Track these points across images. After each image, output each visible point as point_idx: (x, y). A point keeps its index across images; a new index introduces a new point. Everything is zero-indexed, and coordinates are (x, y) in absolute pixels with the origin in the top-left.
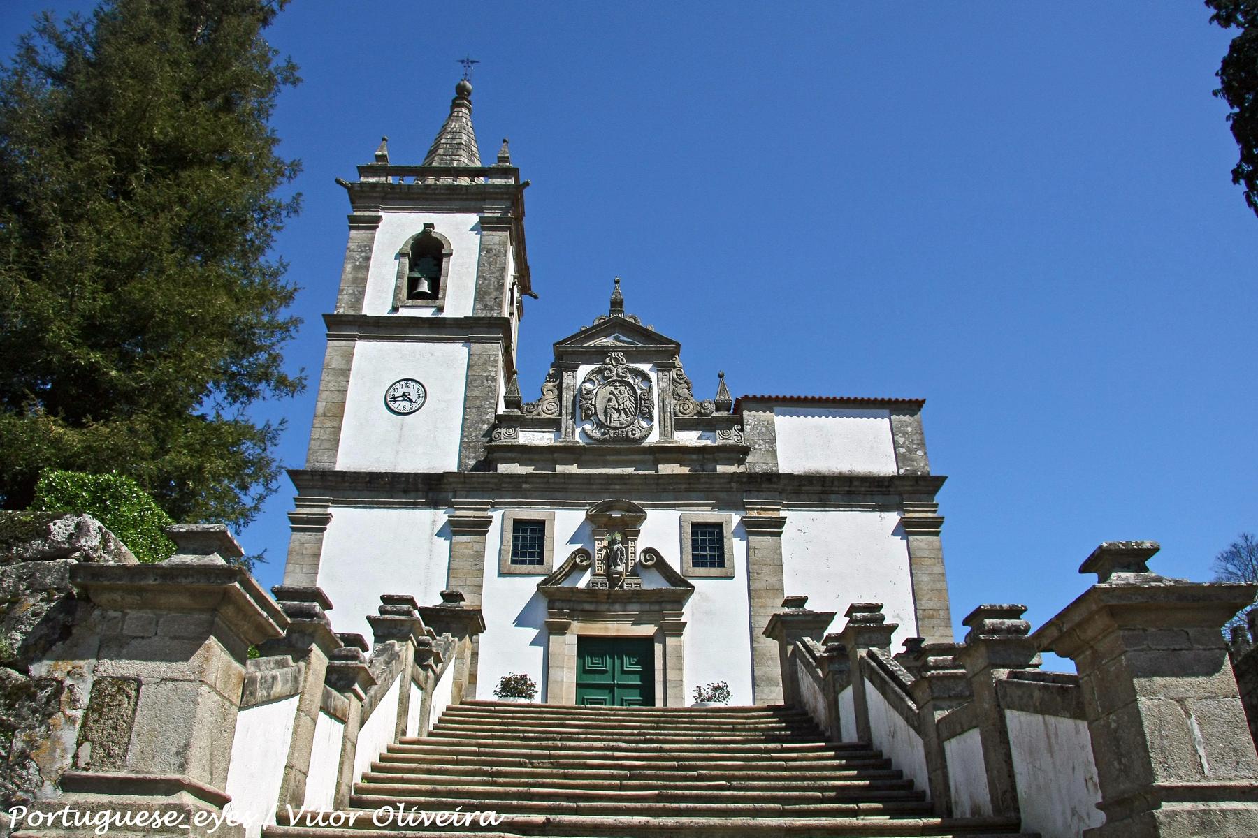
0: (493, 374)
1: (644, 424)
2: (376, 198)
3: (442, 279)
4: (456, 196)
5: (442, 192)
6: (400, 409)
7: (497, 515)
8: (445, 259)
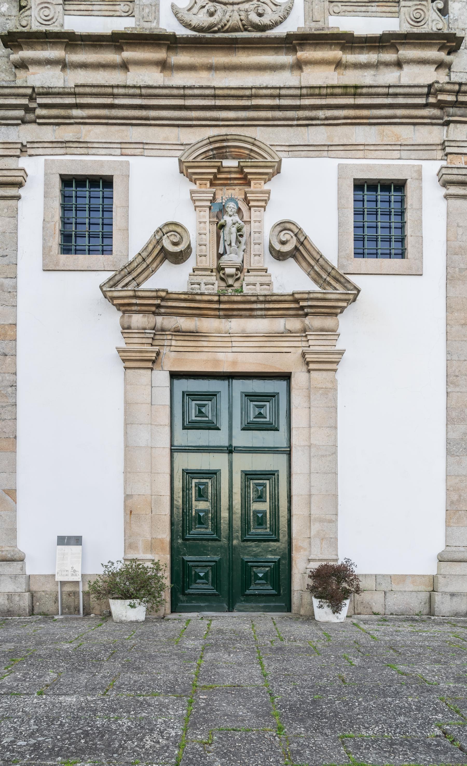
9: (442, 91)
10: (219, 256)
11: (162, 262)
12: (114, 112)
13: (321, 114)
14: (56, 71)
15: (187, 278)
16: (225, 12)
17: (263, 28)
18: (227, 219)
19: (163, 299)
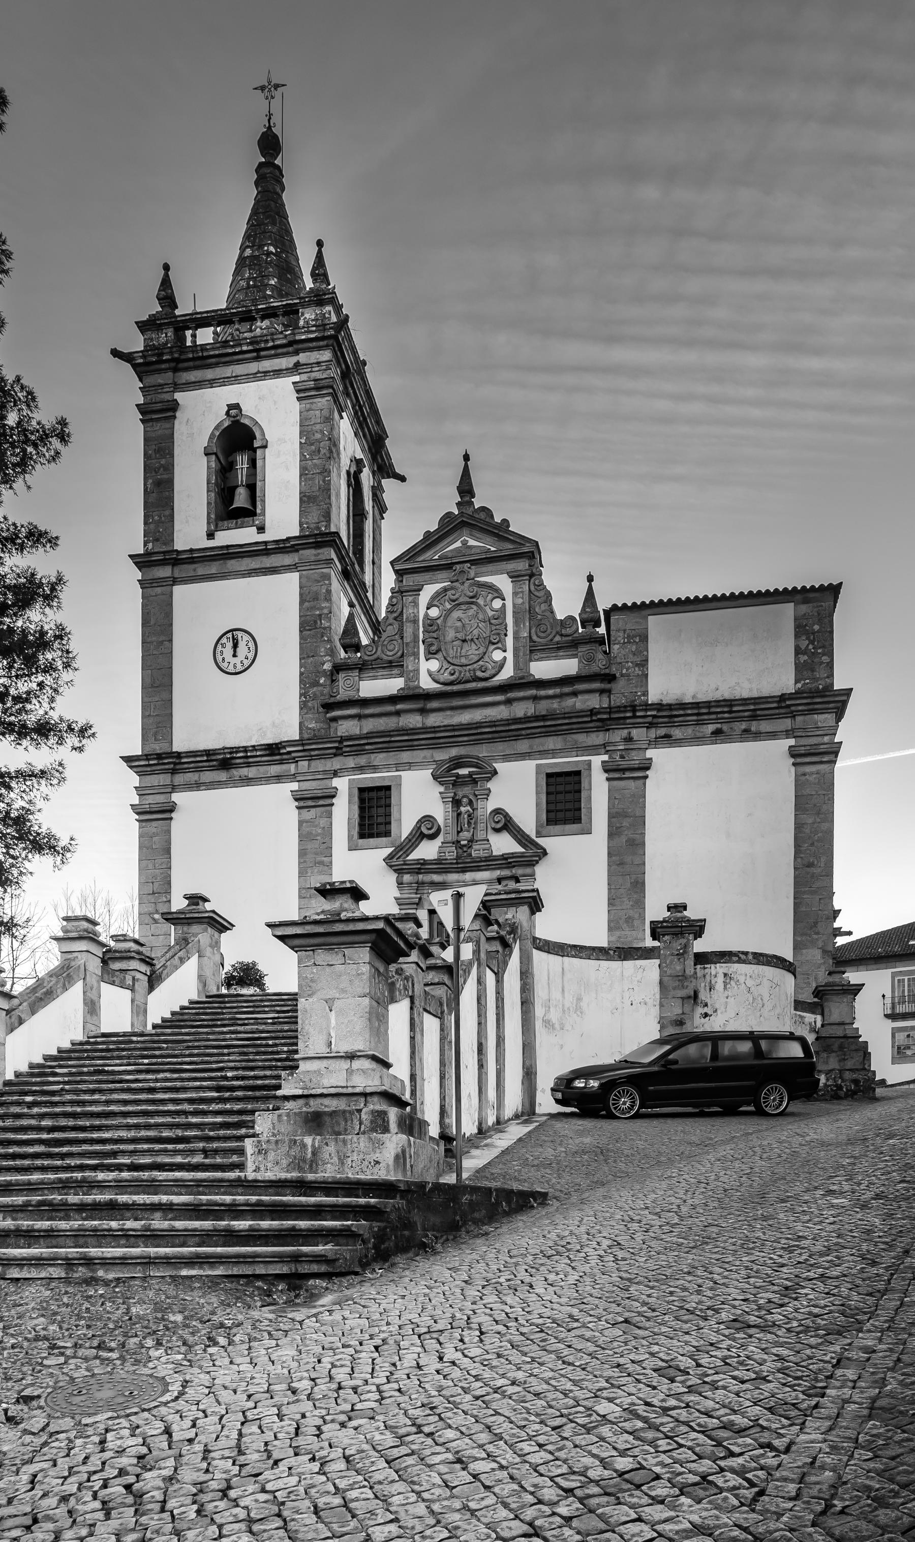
0: (326, 611)
1: (497, 655)
7: (342, 784)
8: (259, 452)
9: (599, 713)
10: (458, 832)
11: (422, 840)
12: (392, 745)
13: (523, 732)
14: (355, 722)
15: (437, 849)
16: (460, 672)
17: (486, 679)
18: (463, 809)
19: (422, 864)
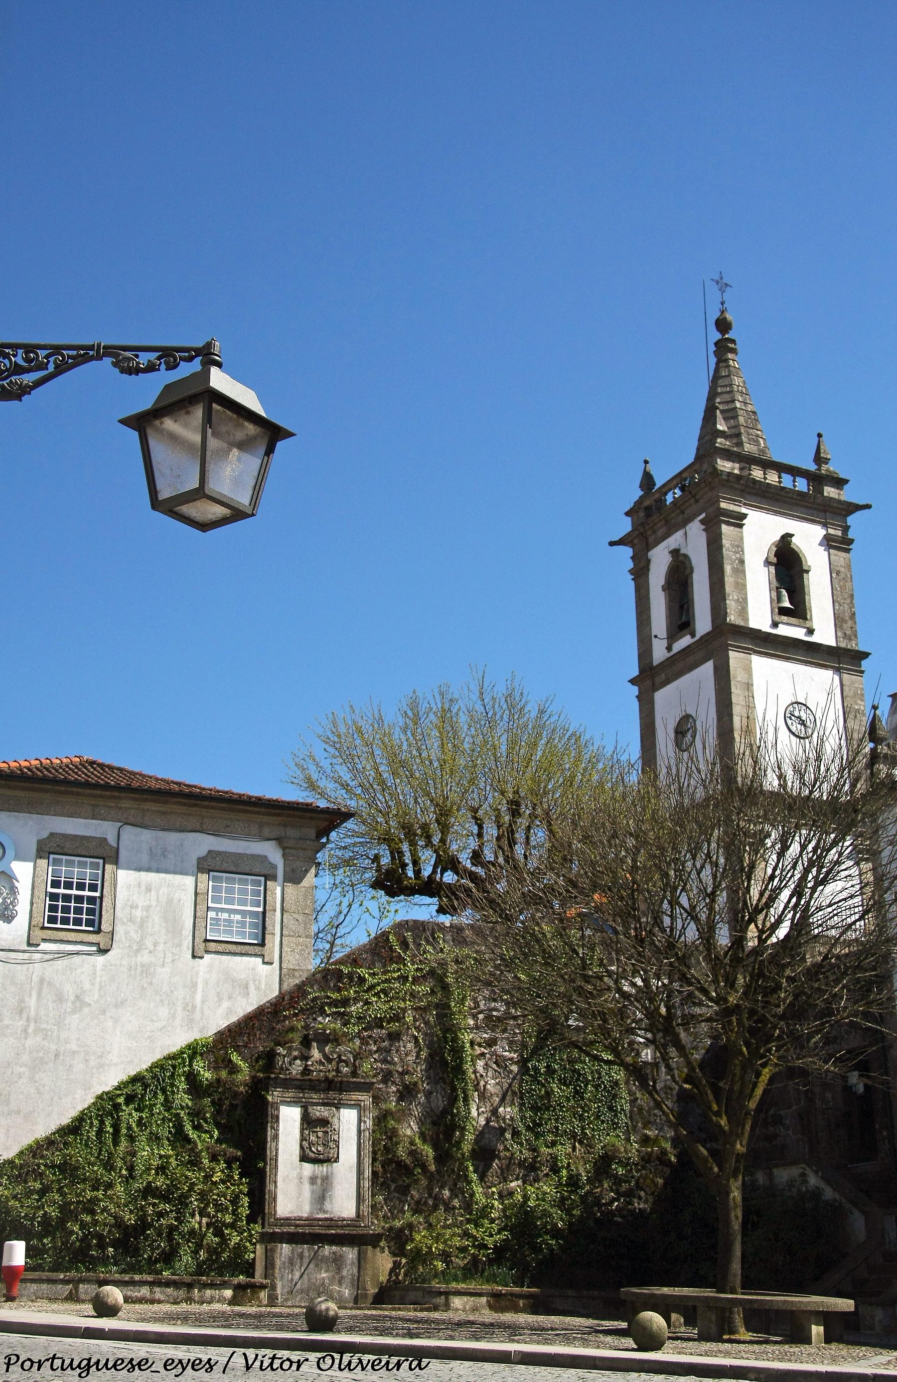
0: (862, 708)
2: (736, 489)
3: (807, 597)
4: (803, 503)
5: (794, 496)
6: (793, 729)
